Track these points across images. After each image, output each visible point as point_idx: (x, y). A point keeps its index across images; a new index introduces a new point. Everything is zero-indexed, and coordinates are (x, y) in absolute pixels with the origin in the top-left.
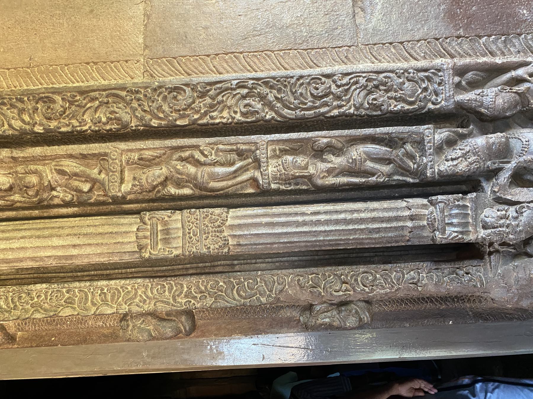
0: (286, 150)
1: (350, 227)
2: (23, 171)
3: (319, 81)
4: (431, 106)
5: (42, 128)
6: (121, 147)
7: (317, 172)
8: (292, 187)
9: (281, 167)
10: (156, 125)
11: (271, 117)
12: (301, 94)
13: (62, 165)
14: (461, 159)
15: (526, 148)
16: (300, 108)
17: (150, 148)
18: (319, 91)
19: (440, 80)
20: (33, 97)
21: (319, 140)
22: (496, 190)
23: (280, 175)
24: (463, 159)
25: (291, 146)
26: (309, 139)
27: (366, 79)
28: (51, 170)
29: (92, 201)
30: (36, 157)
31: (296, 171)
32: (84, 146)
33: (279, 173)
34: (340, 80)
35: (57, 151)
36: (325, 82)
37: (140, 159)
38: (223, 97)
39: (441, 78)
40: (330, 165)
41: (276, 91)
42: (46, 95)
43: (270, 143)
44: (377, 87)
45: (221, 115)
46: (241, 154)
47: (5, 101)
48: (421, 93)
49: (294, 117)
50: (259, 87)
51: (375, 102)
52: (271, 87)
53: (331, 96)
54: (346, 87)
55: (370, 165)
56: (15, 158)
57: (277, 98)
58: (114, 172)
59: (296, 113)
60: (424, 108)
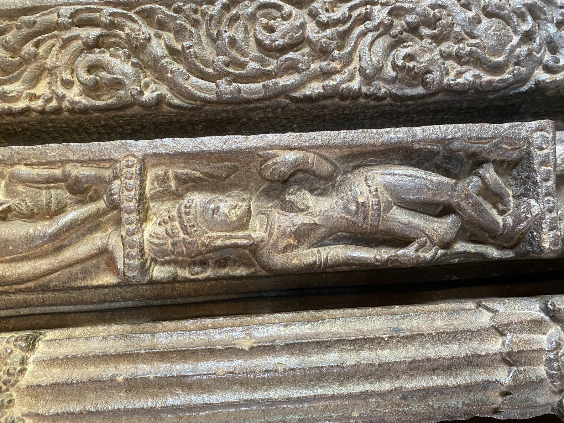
0: (194, 180)
1: (355, 388)
3: (275, 13)
4: (541, 75)
7: (270, 235)
8: (209, 273)
9: (176, 223)
11: (155, 94)
12: (233, 42)
16: (228, 74)
18: (277, 34)
21: (276, 156)
23: (173, 244)
25: (207, 170)
26: (251, 152)
27: (388, 9)
31: (215, 234)
33: (170, 241)
34: (327, 10)
36: (290, 15)
38: (37, 45)
40: (301, 219)
41: (172, 35)
43: (150, 162)
44: (413, 29)
45: (32, 91)
46: (81, 190)
48: (518, 45)
49: (213, 97)
50: (130, 24)
51: (411, 64)
52: (162, 25)
53: (306, 50)
54: (341, 28)
55: (400, 217)
57: (173, 51)
59: (217, 85)
60: (525, 80)
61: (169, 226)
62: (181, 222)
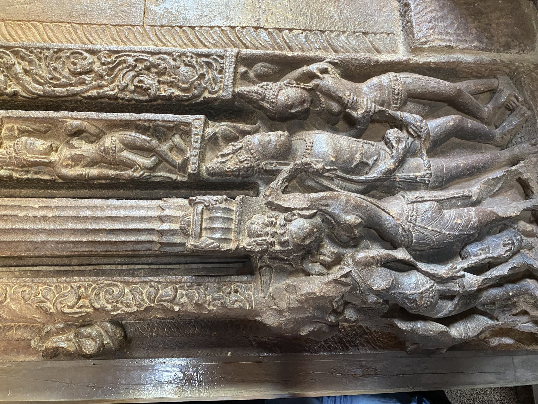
0: (28, 131)
3: (80, 56)
4: (206, 95)
7: (60, 159)
8: (29, 176)
9: (12, 149)
11: (12, 90)
12: (55, 69)
14: (231, 156)
15: (309, 150)
16: (50, 83)
18: (78, 66)
19: (221, 67)
21: (66, 122)
22: (268, 194)
24: (235, 156)
25: (34, 127)
26: (55, 119)
27: (135, 58)
31: (30, 155)
33: (8, 157)
34: (105, 57)
36: (86, 58)
39: (222, 65)
40: (74, 152)
41: (27, 63)
43: (6, 120)
44: (148, 69)
48: (197, 80)
49: (41, 93)
50: (6, 56)
51: (141, 85)
52: (23, 58)
53: (93, 75)
54: (110, 66)
55: (126, 155)
57: (26, 71)
60: (199, 96)
61: (8, 150)
62: (14, 148)
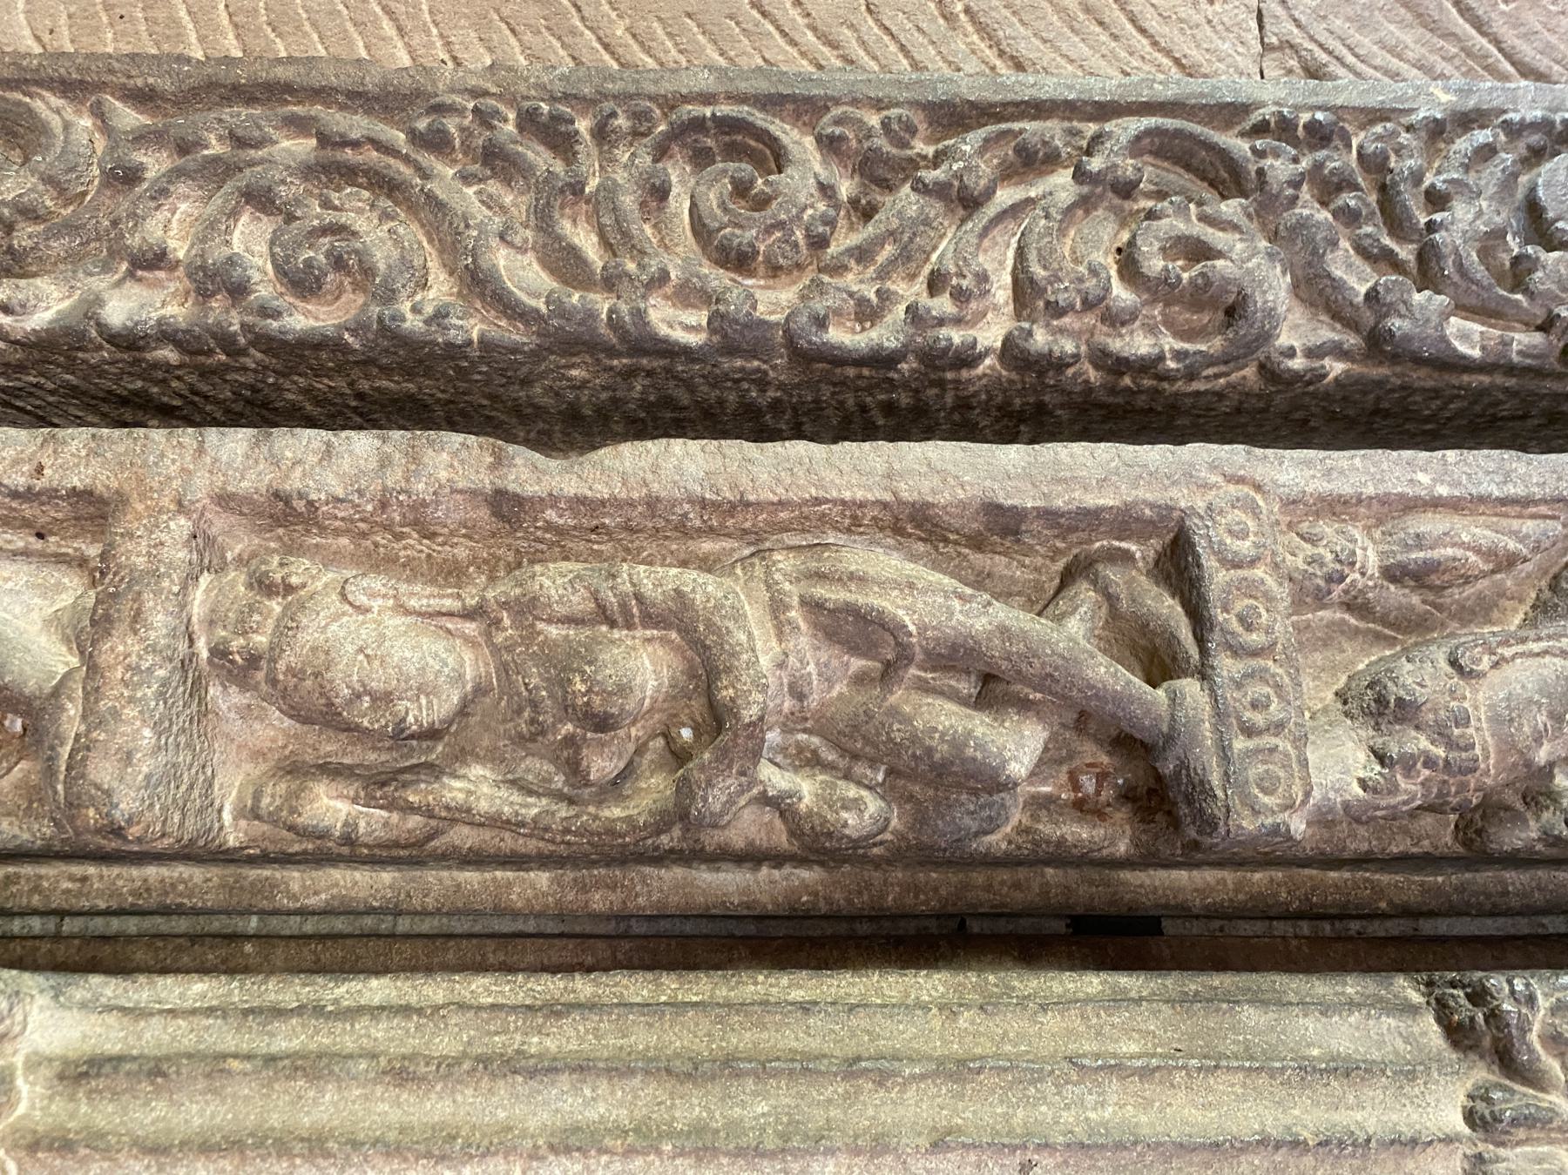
2: (579, 602)
5: (700, 317)
6: (1282, 478)
10: (1476, 353)
13: (861, 580)
17: (1482, 499)
20: (639, 116)
28: (777, 607)
29: (997, 841)
30: (674, 503)
32: (1013, 455)
35: (829, 475)
37: (1393, 574)
42: (724, 109)
47: (451, 125)
56: (519, 500)
58: (1255, 653)
